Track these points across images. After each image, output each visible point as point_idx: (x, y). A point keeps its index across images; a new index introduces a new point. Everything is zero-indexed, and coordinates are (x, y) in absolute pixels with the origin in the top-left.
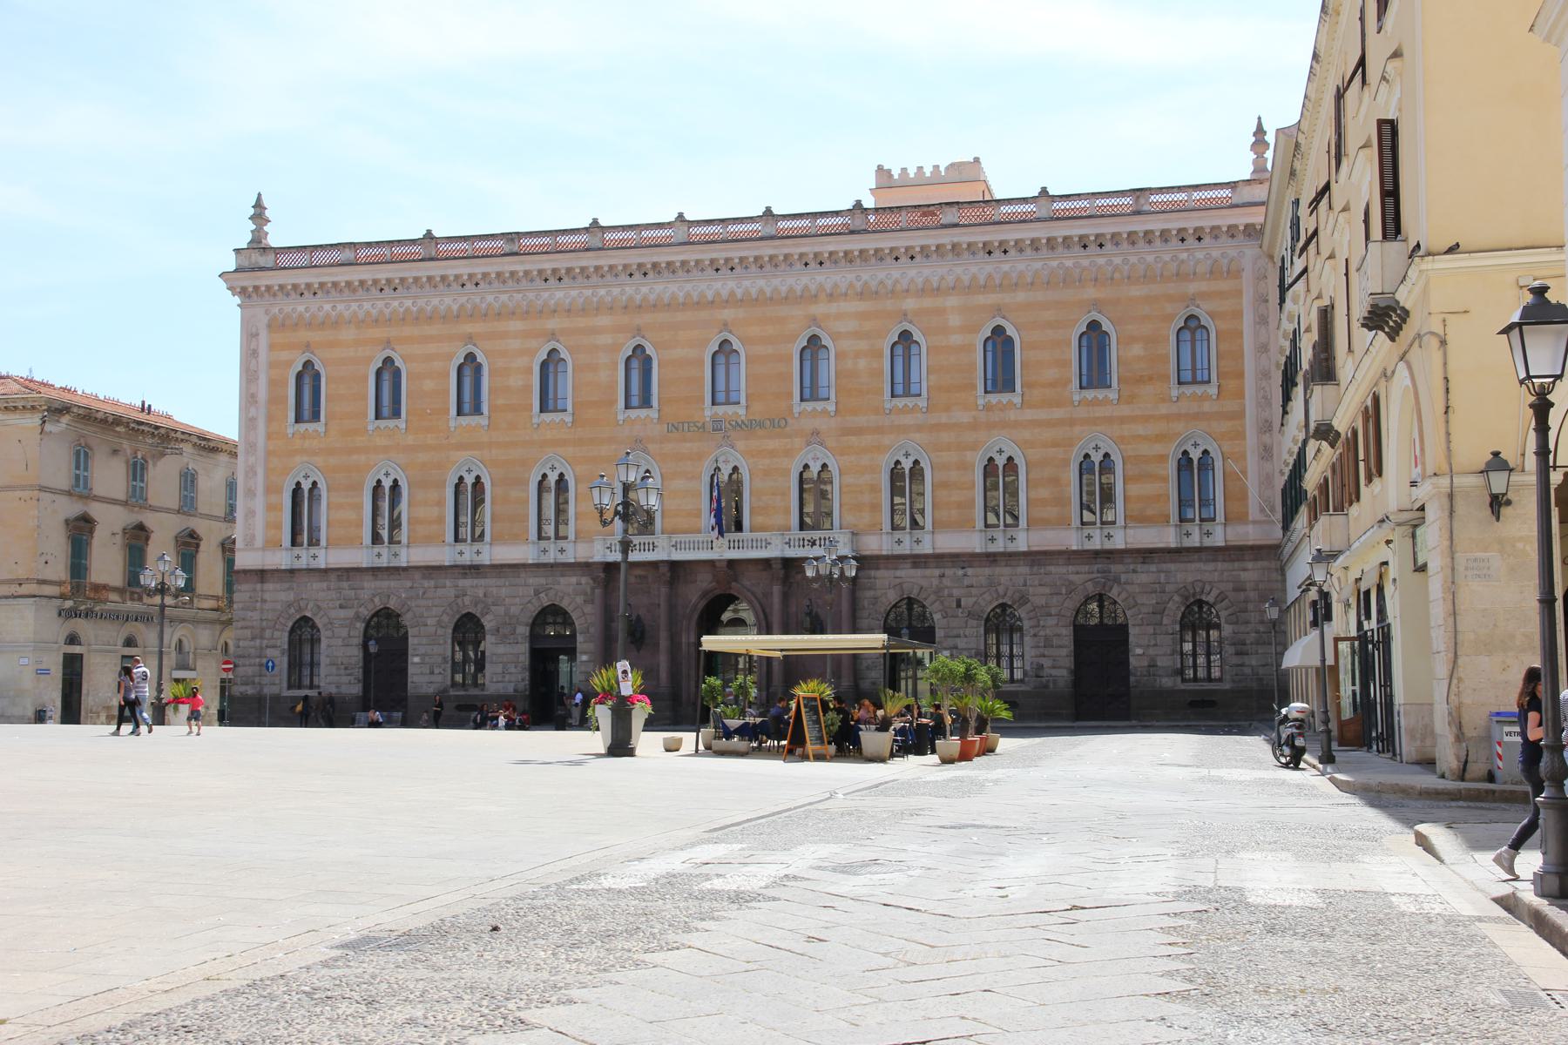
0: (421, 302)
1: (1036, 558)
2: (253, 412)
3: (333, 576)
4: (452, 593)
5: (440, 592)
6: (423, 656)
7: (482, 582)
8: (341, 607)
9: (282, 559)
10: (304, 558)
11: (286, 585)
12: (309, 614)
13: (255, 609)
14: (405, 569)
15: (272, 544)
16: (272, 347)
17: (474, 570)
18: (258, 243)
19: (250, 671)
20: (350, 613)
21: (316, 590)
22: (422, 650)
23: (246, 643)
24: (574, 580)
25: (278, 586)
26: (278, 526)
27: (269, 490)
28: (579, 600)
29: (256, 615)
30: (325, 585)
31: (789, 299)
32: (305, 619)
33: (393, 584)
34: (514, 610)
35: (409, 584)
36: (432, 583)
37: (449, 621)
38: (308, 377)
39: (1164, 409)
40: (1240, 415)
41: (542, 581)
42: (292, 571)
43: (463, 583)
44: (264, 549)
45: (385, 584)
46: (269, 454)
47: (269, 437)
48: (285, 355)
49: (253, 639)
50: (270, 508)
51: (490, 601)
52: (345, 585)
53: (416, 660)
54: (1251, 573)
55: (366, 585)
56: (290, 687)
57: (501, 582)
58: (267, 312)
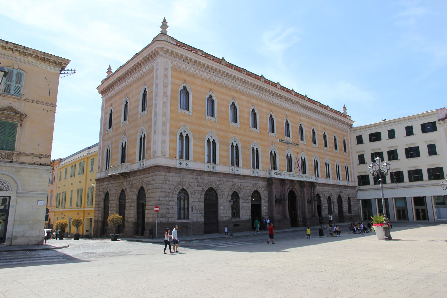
0: (221, 80)
1: (333, 186)
2: (165, 99)
3: (195, 173)
4: (232, 184)
5: (228, 183)
6: (224, 206)
7: (240, 181)
8: (198, 186)
9: (175, 163)
10: (184, 164)
11: (178, 175)
12: (185, 188)
13: (166, 184)
14: (219, 173)
15: (172, 157)
16: (172, 76)
17: (238, 176)
18: (164, 33)
19: (164, 211)
20: (201, 188)
21: (189, 178)
22: (224, 204)
23: (163, 199)
24: (261, 182)
25: (174, 174)
26: (175, 149)
27: (171, 133)
28: (263, 189)
29: (166, 186)
30: (192, 176)
31: (299, 114)
32: (183, 190)
33: (214, 178)
34: (248, 191)
35: (219, 179)
36: (226, 179)
37: (231, 193)
38: (185, 92)
39: (343, 157)
40: (350, 160)
41: (254, 182)
42: (181, 169)
43: (235, 180)
44: (169, 158)
45: (212, 178)
46: (171, 118)
47: (171, 111)
48: (177, 81)
49: (165, 197)
50: (171, 141)
51: (242, 187)
52: (199, 177)
53: (222, 208)
54: (354, 191)
55: (206, 178)
56: (179, 218)
57: (244, 181)
58: (172, 62)
